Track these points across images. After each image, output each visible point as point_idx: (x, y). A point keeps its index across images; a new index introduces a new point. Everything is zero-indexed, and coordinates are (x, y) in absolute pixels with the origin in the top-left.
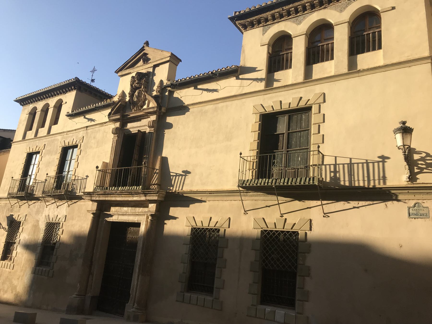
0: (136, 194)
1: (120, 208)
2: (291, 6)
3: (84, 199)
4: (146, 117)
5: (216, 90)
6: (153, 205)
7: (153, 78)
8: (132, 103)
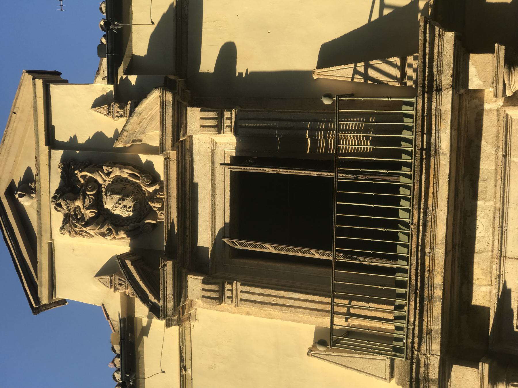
1: (476, 255)
4: (188, 158)
6: (472, 70)
7: (81, 147)
8: (136, 228)
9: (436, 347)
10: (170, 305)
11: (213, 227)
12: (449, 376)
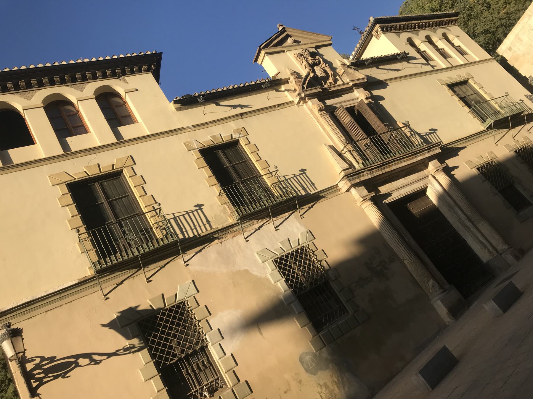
0: (420, 152)
2: (409, 22)
3: (324, 197)
4: (347, 92)
5: (398, 70)
6: (434, 161)
9: (370, 176)
10: (308, 93)
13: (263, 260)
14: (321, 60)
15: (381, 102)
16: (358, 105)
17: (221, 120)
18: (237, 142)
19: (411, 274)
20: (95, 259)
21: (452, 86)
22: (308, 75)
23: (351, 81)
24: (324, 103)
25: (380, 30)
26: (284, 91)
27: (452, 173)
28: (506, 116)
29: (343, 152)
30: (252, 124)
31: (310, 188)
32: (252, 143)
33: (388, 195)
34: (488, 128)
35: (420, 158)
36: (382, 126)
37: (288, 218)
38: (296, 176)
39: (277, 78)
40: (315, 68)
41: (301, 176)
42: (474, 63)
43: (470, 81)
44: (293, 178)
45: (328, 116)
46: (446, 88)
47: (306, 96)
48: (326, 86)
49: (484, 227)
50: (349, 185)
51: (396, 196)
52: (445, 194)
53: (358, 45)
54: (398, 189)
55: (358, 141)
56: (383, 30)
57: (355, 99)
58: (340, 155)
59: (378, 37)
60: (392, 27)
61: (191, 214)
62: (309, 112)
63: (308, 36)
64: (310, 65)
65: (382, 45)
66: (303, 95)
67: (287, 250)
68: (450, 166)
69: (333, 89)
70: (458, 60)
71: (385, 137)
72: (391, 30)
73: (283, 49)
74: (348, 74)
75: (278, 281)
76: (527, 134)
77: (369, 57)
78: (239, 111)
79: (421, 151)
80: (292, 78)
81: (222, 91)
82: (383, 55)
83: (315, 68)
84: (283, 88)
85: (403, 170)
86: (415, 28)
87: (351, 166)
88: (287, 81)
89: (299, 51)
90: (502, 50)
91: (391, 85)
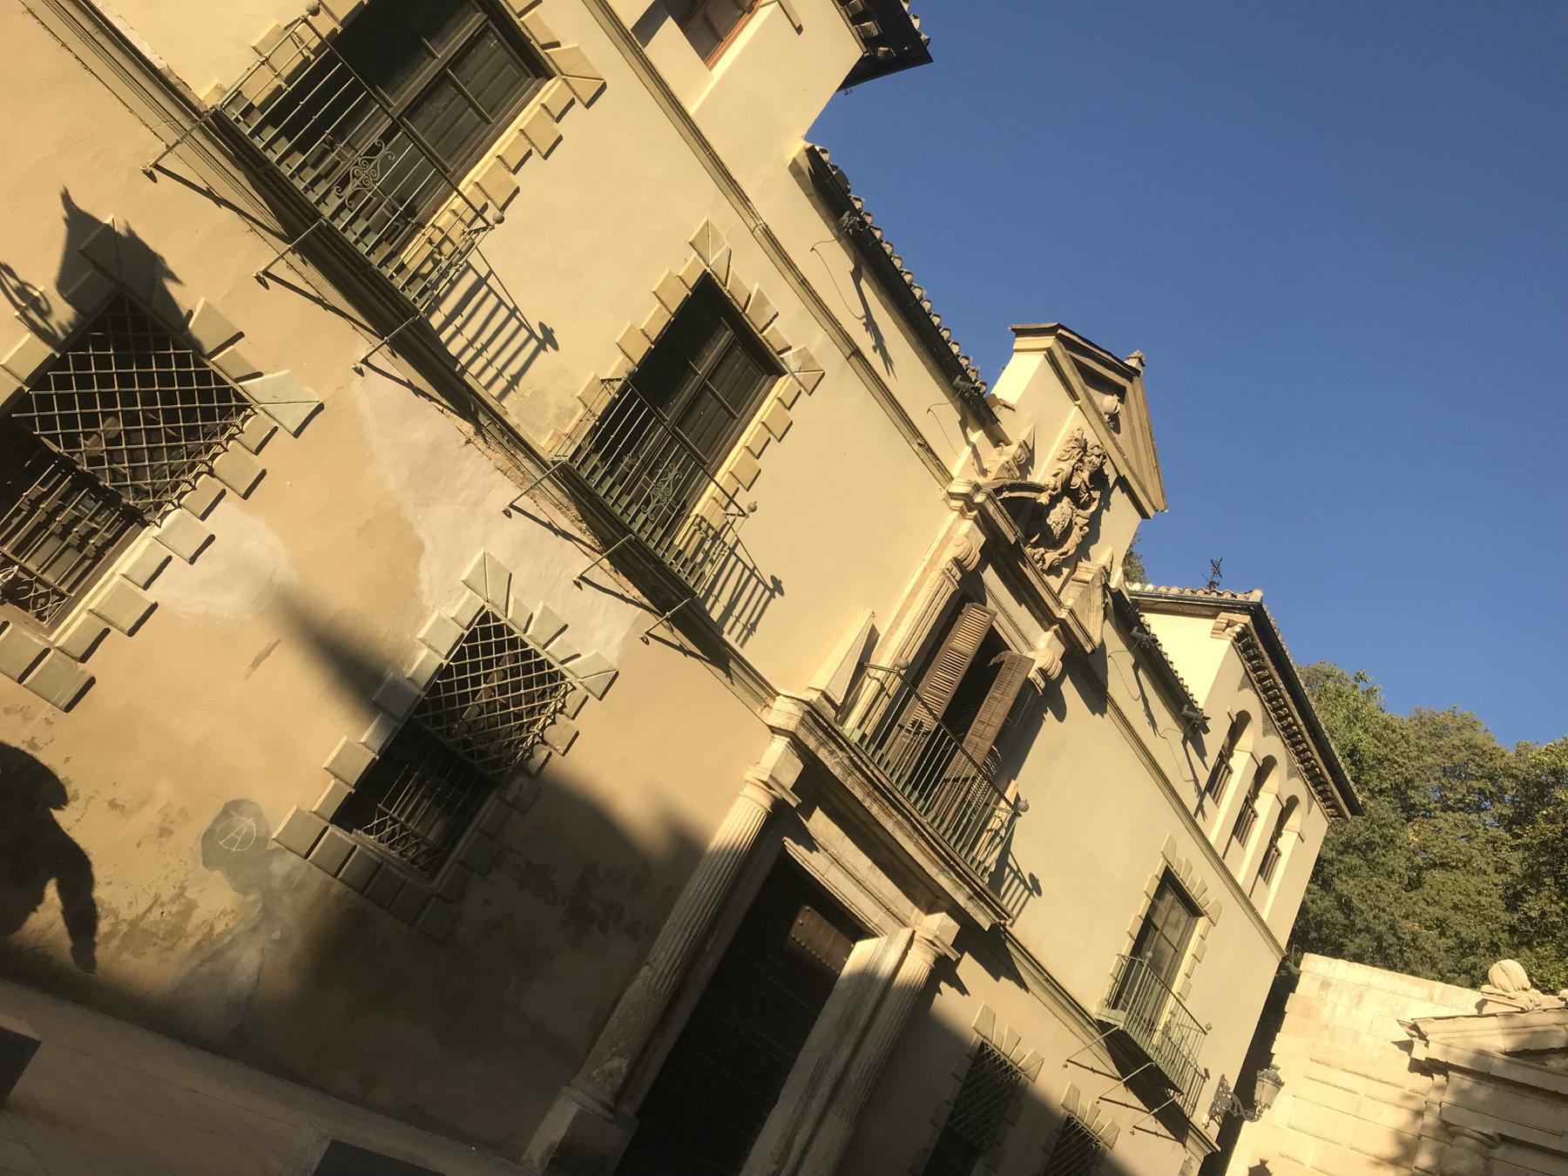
2: (1287, 696)
3: (729, 675)
4: (1038, 614)
5: (1153, 723)
6: (952, 923)
9: (837, 772)
10: (991, 508)
11: (993, 596)
12: (799, 757)
13: (472, 583)
14: (1093, 508)
15: (1049, 716)
16: (1015, 657)
17: (818, 301)
18: (777, 371)
19: (617, 1001)
20: (257, 93)
21: (1169, 882)
22: (1040, 489)
23: (1071, 612)
24: (981, 566)
25: (1238, 629)
26: (968, 443)
27: (943, 986)
28: (1150, 1052)
29: (872, 672)
30: (844, 391)
31: (739, 627)
32: (792, 415)
33: (810, 844)
34: (1100, 1022)
35: (944, 881)
36: (987, 745)
37: (627, 601)
38: (752, 573)
39: (996, 410)
40: (1066, 500)
41: (761, 587)
42: (1252, 909)
43: (1202, 922)
44: (746, 566)
45: (952, 589)
46: (1158, 870)
47: (981, 508)
48: (1028, 550)
49: (835, 1131)
50: (791, 728)
51: (815, 864)
52: (876, 994)
53: (1174, 591)
54: (836, 860)
55: (919, 699)
56: (1239, 637)
57: (1027, 642)
58: (861, 668)
59: (1217, 632)
60: (1258, 657)
61: (514, 324)
62: (941, 535)
63: (1141, 446)
64: (1067, 483)
65: (1199, 651)
66: (979, 498)
67: (533, 637)
68: (959, 971)
69: (1028, 572)
70: (1244, 863)
71: (959, 766)
72: (1249, 659)
73: (1080, 393)
74: (1085, 597)
75: (430, 647)
76: (1125, 1128)
77: (1153, 631)
78: (865, 342)
79: (964, 878)
80: (1013, 450)
81: (898, 273)
82: (1175, 667)
83: (1066, 500)
84: (977, 436)
85: (892, 852)
86: (1280, 719)
87: (844, 710)
88: (998, 439)
89: (1092, 439)
90: (1314, 966)
91: (1105, 724)
